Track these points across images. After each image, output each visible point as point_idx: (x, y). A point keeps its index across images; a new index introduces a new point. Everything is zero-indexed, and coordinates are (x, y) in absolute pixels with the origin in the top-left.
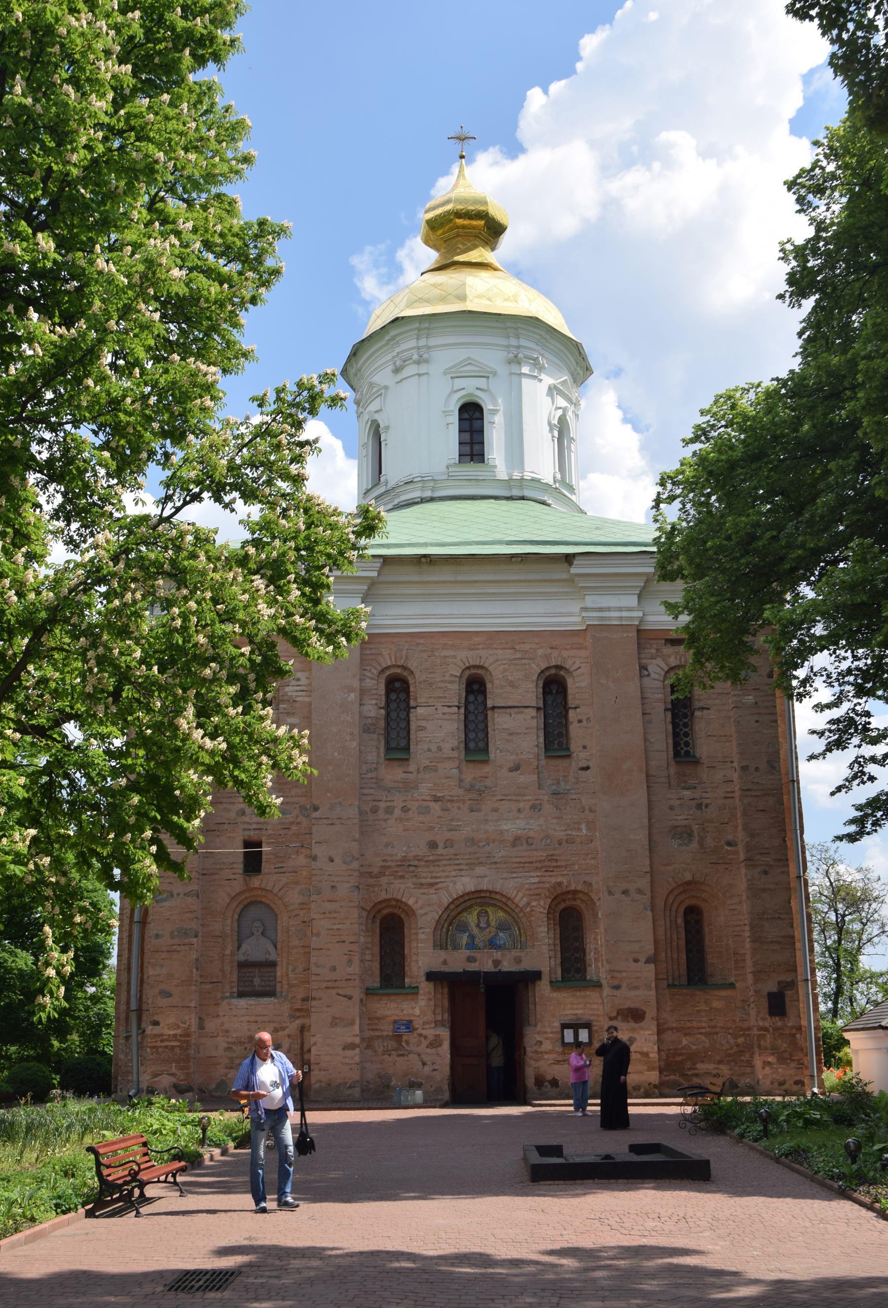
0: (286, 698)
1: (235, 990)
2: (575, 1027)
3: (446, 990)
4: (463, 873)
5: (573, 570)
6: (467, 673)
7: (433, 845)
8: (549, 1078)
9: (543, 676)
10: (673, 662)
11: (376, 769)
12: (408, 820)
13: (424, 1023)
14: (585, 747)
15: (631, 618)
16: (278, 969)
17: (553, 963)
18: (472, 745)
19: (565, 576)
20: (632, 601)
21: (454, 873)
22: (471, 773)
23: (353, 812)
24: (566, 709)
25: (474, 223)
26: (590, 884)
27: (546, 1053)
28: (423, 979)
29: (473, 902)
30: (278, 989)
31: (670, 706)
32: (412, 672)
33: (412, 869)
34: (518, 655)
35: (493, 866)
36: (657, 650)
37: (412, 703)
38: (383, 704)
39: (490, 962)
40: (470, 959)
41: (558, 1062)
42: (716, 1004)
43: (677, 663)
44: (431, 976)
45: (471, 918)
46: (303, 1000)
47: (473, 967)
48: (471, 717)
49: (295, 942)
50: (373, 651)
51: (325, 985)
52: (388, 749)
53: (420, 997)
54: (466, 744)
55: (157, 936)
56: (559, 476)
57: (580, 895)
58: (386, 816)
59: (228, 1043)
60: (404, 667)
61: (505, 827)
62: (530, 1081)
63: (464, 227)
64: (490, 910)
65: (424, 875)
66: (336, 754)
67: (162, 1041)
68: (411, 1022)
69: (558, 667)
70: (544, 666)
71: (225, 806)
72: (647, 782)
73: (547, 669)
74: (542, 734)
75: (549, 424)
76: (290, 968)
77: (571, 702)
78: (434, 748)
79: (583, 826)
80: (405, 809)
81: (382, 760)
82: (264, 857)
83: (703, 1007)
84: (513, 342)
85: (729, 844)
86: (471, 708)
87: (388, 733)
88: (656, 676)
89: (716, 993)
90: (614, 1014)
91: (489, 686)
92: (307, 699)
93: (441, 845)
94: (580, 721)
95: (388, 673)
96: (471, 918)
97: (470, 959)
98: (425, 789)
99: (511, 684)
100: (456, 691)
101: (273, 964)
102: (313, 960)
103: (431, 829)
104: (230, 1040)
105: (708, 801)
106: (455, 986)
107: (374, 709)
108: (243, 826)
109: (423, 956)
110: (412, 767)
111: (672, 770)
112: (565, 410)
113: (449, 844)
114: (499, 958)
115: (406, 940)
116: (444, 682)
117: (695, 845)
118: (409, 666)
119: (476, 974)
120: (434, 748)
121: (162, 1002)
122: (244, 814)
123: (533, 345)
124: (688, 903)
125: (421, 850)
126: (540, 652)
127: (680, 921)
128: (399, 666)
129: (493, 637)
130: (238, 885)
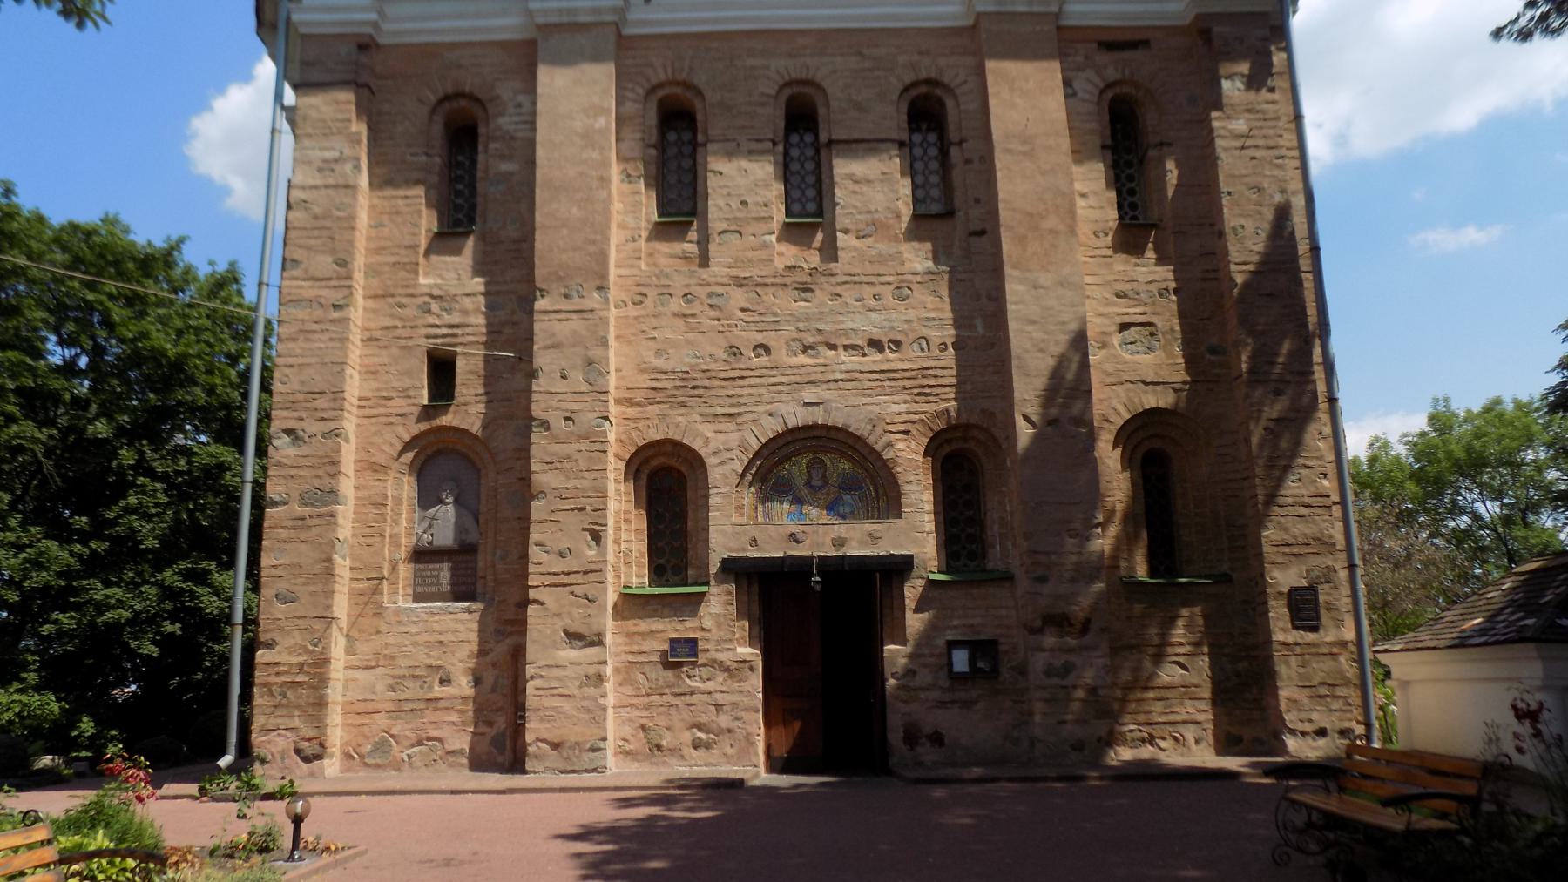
0: (498, 133)
3: (755, 588)
4: (785, 397)
6: (787, 92)
7: (734, 351)
8: (928, 729)
10: (1112, 74)
12: (693, 316)
13: (720, 641)
14: (977, 201)
18: (796, 207)
26: (993, 414)
27: (922, 689)
31: (1109, 142)
32: (699, 93)
33: (701, 391)
34: (867, 64)
35: (832, 385)
36: (1086, 58)
37: (700, 138)
39: (828, 541)
41: (943, 704)
43: (1118, 76)
45: (797, 470)
48: (795, 167)
55: (275, 504)
57: (975, 433)
59: (394, 677)
60: (685, 85)
61: (851, 325)
62: (895, 737)
64: (827, 458)
66: (574, 211)
67: (277, 674)
68: (694, 641)
69: (929, 82)
70: (908, 78)
71: (398, 299)
73: (915, 84)
76: (499, 552)
77: (953, 135)
79: (979, 323)
82: (459, 379)
85: (1213, 351)
86: (795, 153)
87: (664, 177)
88: (1087, 96)
90: (1038, 623)
91: (821, 111)
94: (968, 161)
95: (661, 93)
99: (859, 107)
100: (773, 118)
102: (534, 536)
104: (397, 672)
108: (424, 331)
115: (690, 508)
118: (696, 81)
119: (806, 562)
121: (280, 610)
122: (429, 311)
126: (902, 59)
128: (678, 84)
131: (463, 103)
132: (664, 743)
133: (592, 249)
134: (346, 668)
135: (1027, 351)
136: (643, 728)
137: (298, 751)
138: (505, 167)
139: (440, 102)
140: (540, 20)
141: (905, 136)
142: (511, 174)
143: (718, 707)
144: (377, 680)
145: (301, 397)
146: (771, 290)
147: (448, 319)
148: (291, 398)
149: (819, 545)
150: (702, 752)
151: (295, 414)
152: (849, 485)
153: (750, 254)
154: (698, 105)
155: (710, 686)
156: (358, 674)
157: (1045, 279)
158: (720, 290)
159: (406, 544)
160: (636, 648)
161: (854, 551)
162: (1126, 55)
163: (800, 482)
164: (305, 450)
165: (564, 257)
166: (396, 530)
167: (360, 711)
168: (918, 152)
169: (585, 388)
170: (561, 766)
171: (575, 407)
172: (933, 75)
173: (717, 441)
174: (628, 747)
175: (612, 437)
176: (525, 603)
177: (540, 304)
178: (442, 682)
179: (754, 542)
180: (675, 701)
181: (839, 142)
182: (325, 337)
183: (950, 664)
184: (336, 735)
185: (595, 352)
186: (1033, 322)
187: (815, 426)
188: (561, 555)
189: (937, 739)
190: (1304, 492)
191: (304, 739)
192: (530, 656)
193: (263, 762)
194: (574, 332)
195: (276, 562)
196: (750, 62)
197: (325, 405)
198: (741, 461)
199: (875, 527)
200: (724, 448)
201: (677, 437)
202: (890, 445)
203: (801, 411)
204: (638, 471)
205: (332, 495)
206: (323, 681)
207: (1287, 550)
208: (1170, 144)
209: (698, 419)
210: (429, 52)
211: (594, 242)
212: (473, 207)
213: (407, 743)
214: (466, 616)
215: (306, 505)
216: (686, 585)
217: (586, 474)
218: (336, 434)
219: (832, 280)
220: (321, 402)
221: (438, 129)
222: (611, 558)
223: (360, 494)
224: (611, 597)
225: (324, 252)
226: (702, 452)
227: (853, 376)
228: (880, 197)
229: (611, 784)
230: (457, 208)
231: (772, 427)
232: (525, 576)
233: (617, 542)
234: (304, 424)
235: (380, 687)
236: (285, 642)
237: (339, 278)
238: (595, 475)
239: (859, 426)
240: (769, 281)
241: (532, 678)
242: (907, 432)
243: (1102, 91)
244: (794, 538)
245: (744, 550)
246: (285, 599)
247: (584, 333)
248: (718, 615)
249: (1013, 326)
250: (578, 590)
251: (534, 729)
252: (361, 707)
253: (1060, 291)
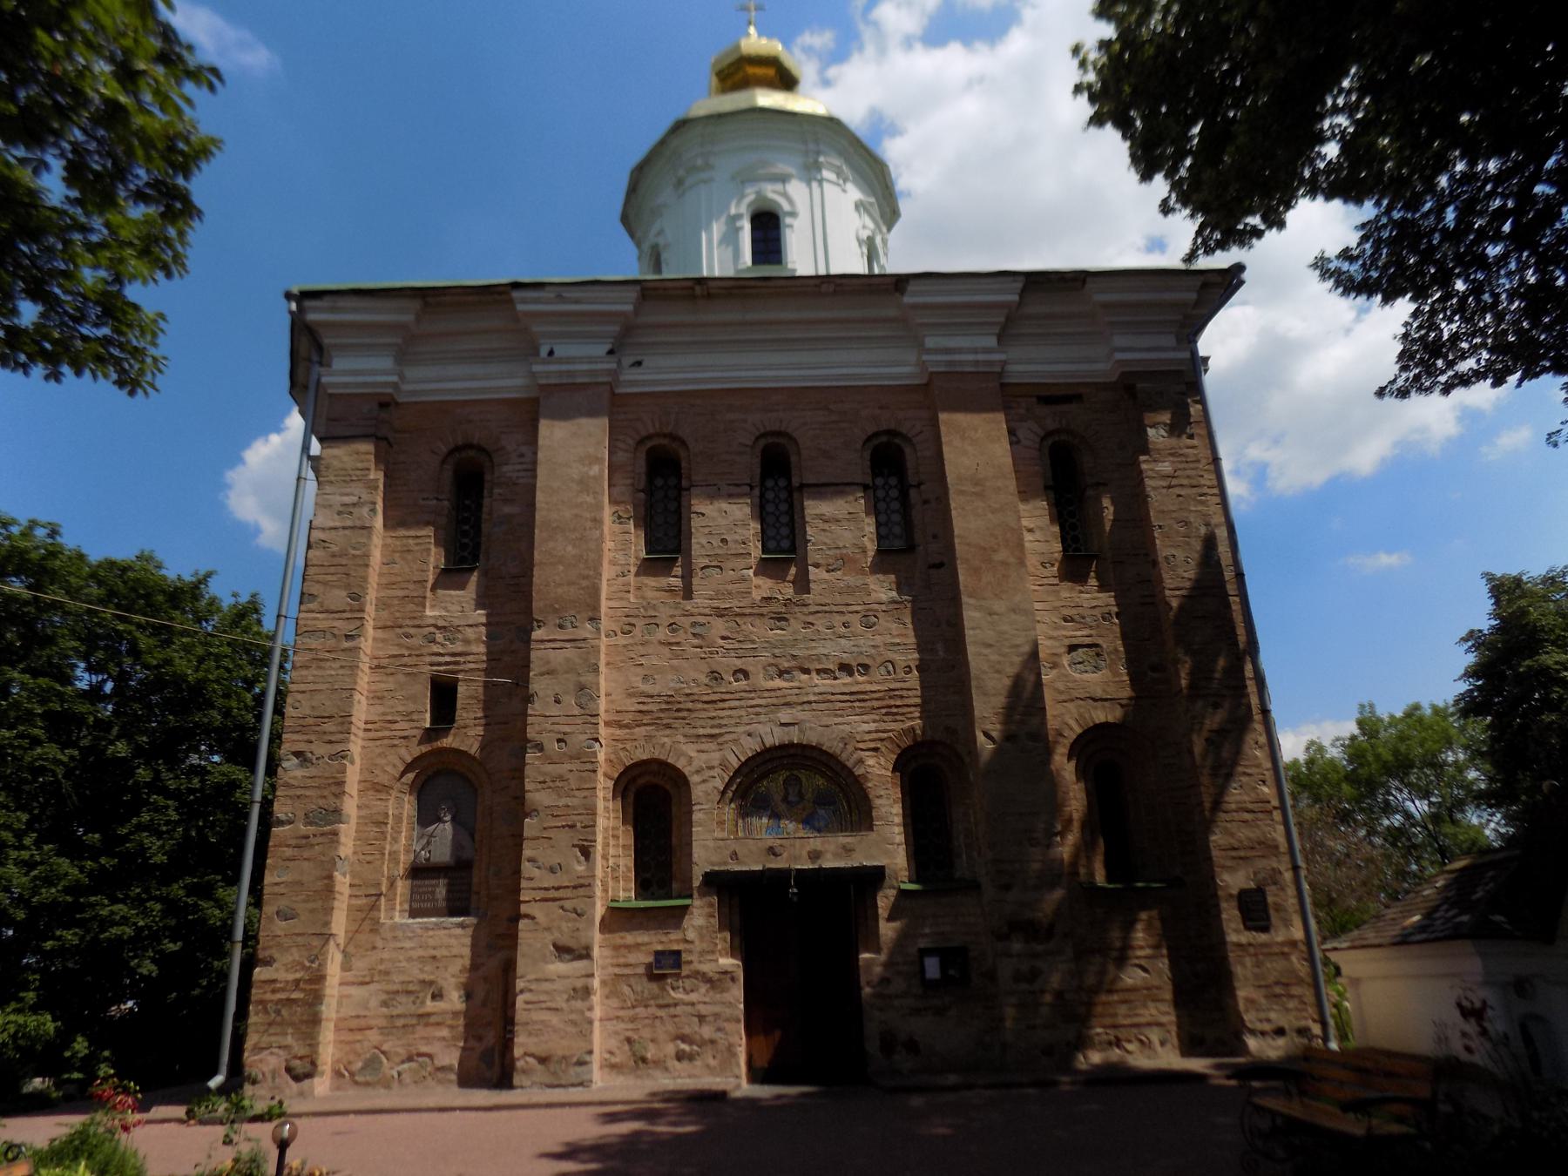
4: (762, 718)
5: (907, 299)
6: (762, 442)
7: (715, 676)
10: (1051, 425)
12: (678, 644)
13: (703, 953)
14: (935, 537)
15: (991, 363)
19: (892, 312)
20: (992, 342)
32: (683, 443)
33: (685, 714)
35: (806, 707)
37: (684, 483)
38: (642, 486)
39: (805, 853)
45: (774, 786)
48: (770, 508)
51: (539, 895)
55: (281, 823)
59: (388, 993)
60: (673, 437)
62: (872, 1047)
64: (802, 775)
66: (570, 548)
67: (273, 991)
68: (678, 953)
70: (871, 429)
73: (876, 435)
77: (912, 480)
79: (939, 646)
86: (770, 495)
91: (793, 459)
94: (926, 502)
95: (649, 444)
100: (750, 465)
102: (527, 853)
108: (428, 659)
114: (819, 848)
119: (782, 876)
121: (280, 926)
122: (434, 641)
128: (665, 436)
129: (797, 396)
131: (472, 453)
132: (649, 1056)
133: (585, 583)
134: (341, 984)
135: (985, 672)
136: (629, 1041)
137: (288, 1070)
138: (507, 509)
139: (451, 453)
140: (543, 381)
141: (869, 481)
143: (702, 1018)
144: (370, 996)
145: (310, 721)
146: (750, 619)
147: (451, 648)
148: (301, 722)
149: (796, 859)
150: (685, 1064)
151: (305, 737)
152: (823, 800)
153: (730, 587)
154: (683, 454)
155: (693, 997)
156: (353, 990)
157: (999, 606)
158: (701, 619)
159: (405, 860)
160: (622, 960)
161: (829, 863)
162: (1065, 407)
163: (778, 798)
164: (312, 771)
165: (560, 590)
166: (395, 848)
167: (353, 1027)
168: (881, 494)
169: (577, 711)
170: (548, 1080)
171: (567, 729)
172: (892, 426)
173: (700, 760)
174: (614, 1060)
175: (601, 757)
176: (516, 917)
177: (537, 634)
178: (434, 997)
179: (735, 856)
180: (660, 1013)
181: (809, 486)
182: (336, 665)
183: (923, 970)
184: (328, 1051)
185: (587, 678)
186: (990, 646)
187: (791, 745)
188: (552, 870)
189: (912, 1046)
190: (1246, 798)
191: (295, 1057)
192: (520, 970)
193: (254, 1082)
194: (568, 660)
195: (278, 880)
197: (333, 729)
198: (722, 779)
199: (849, 840)
200: (706, 767)
201: (662, 757)
202: (861, 761)
203: (778, 731)
204: (626, 789)
205: (336, 814)
206: (316, 998)
207: (1234, 854)
208: (1105, 485)
209: (681, 739)
210: (443, 408)
211: (586, 577)
212: (478, 545)
213: (397, 1060)
214: (459, 931)
215: (311, 824)
216: (671, 898)
217: (577, 793)
218: (342, 756)
219: (805, 609)
220: (329, 726)
221: (448, 475)
222: (599, 872)
223: (364, 812)
224: (599, 911)
225: (339, 587)
226: (686, 771)
227: (825, 698)
228: (847, 534)
229: (596, 1098)
230: (464, 547)
231: (751, 746)
232: (518, 890)
233: (605, 857)
234: (313, 747)
235: (374, 1003)
236: (283, 959)
237: (351, 611)
238: (586, 793)
239: (831, 744)
240: (748, 611)
241: (522, 992)
242: (876, 750)
243: (1043, 439)
244: (772, 851)
245: (725, 863)
246: (284, 915)
247: (577, 660)
248: (701, 927)
249: (971, 650)
250: (568, 904)
251: (523, 1043)
252: (354, 1024)
253: (1013, 616)
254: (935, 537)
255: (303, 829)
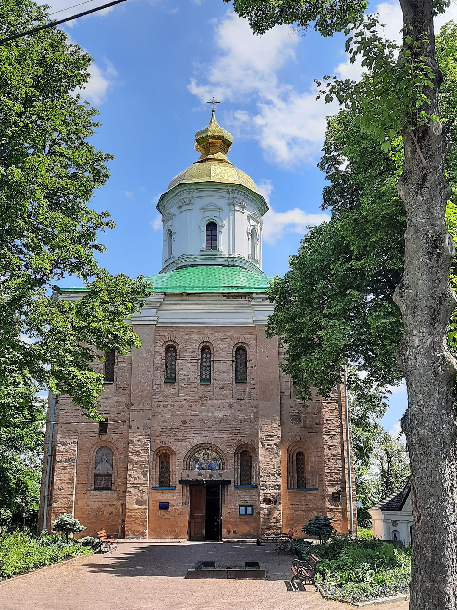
1: (93, 487)
2: (246, 506)
4: (197, 435)
6: (202, 344)
7: (184, 422)
9: (236, 347)
11: (160, 387)
14: (253, 379)
16: (113, 477)
17: (236, 477)
18: (204, 377)
21: (193, 435)
22: (202, 390)
23: (148, 406)
24: (246, 361)
25: (217, 141)
28: (178, 483)
29: (201, 448)
30: (112, 487)
33: (175, 432)
35: (211, 432)
37: (178, 358)
39: (208, 475)
40: (199, 474)
42: (309, 497)
44: (181, 482)
45: (200, 455)
46: (123, 492)
47: (200, 478)
48: (204, 364)
49: (121, 465)
50: (160, 334)
52: (167, 378)
53: (176, 491)
54: (201, 377)
55: (58, 462)
56: (251, 256)
58: (164, 409)
61: (216, 414)
63: (213, 143)
65: (180, 435)
72: (280, 395)
74: (234, 372)
75: (247, 232)
78: (186, 378)
79: (252, 415)
80: (172, 406)
81: (163, 383)
83: (304, 498)
84: (231, 195)
85: (317, 424)
89: (308, 492)
92: (130, 355)
93: (188, 422)
94: (251, 367)
96: (200, 455)
97: (199, 474)
98: (181, 397)
101: (111, 475)
102: (129, 473)
103: (183, 414)
104: (89, 510)
105: (308, 404)
106: (192, 486)
107: (159, 360)
109: (178, 472)
110: (176, 387)
111: (292, 390)
112: (255, 226)
113: (191, 421)
116: (192, 348)
117: (301, 424)
120: (186, 378)
123: (240, 197)
124: (298, 450)
125: (179, 424)
126: (235, 336)
127: (295, 458)
130: (96, 438)
142: (124, 367)
147: (105, 409)
161: (215, 478)
164: (67, 447)
171: (141, 437)
176: (125, 492)
190: (338, 466)
196: (193, 335)
219: (212, 401)
234: (66, 440)
250: (140, 489)
254: (253, 379)
255: (65, 465)
